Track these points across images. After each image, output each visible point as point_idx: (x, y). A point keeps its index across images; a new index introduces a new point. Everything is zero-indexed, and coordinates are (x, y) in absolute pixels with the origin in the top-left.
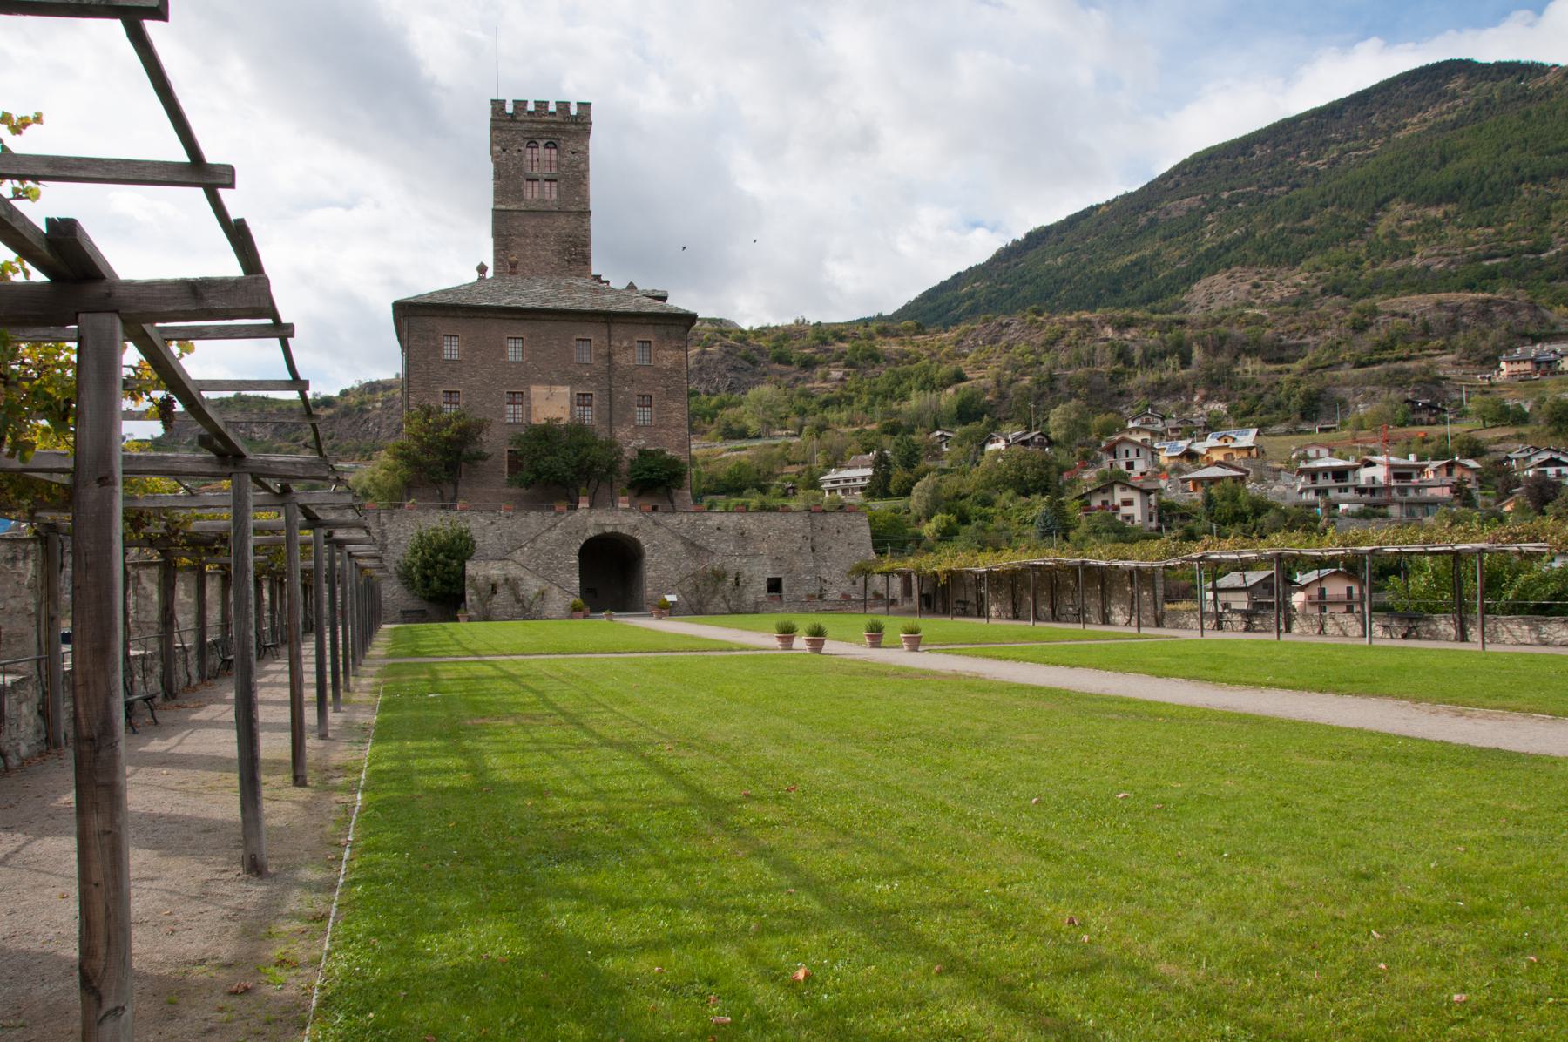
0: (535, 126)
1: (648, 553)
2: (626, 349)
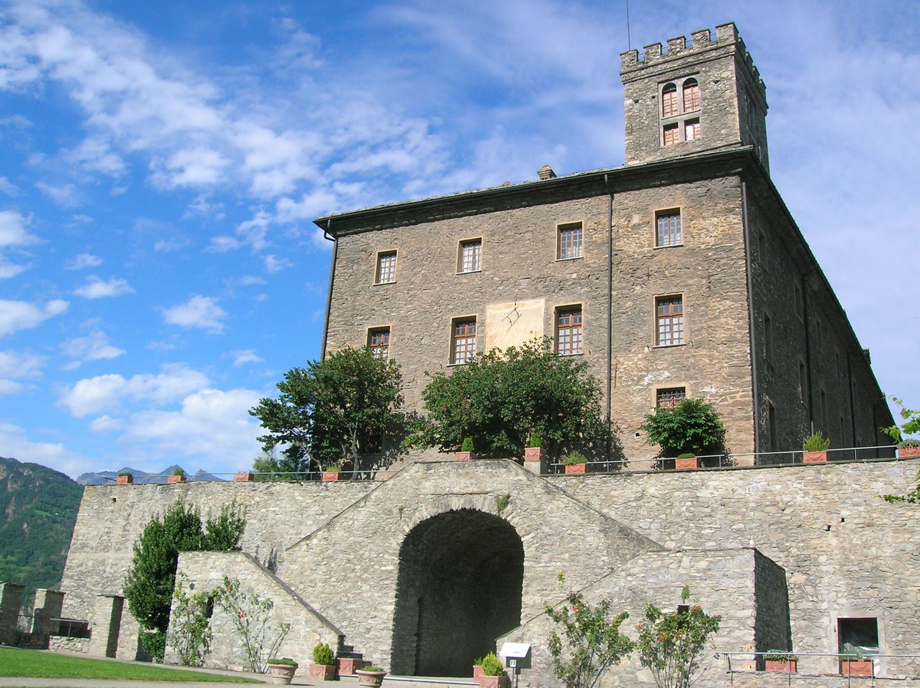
0: (668, 66)
1: (528, 551)
2: (637, 227)
